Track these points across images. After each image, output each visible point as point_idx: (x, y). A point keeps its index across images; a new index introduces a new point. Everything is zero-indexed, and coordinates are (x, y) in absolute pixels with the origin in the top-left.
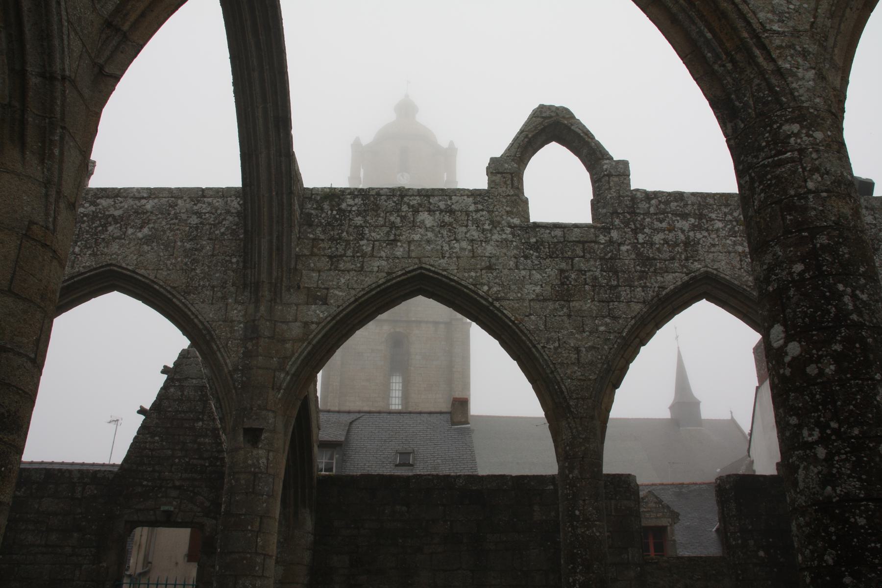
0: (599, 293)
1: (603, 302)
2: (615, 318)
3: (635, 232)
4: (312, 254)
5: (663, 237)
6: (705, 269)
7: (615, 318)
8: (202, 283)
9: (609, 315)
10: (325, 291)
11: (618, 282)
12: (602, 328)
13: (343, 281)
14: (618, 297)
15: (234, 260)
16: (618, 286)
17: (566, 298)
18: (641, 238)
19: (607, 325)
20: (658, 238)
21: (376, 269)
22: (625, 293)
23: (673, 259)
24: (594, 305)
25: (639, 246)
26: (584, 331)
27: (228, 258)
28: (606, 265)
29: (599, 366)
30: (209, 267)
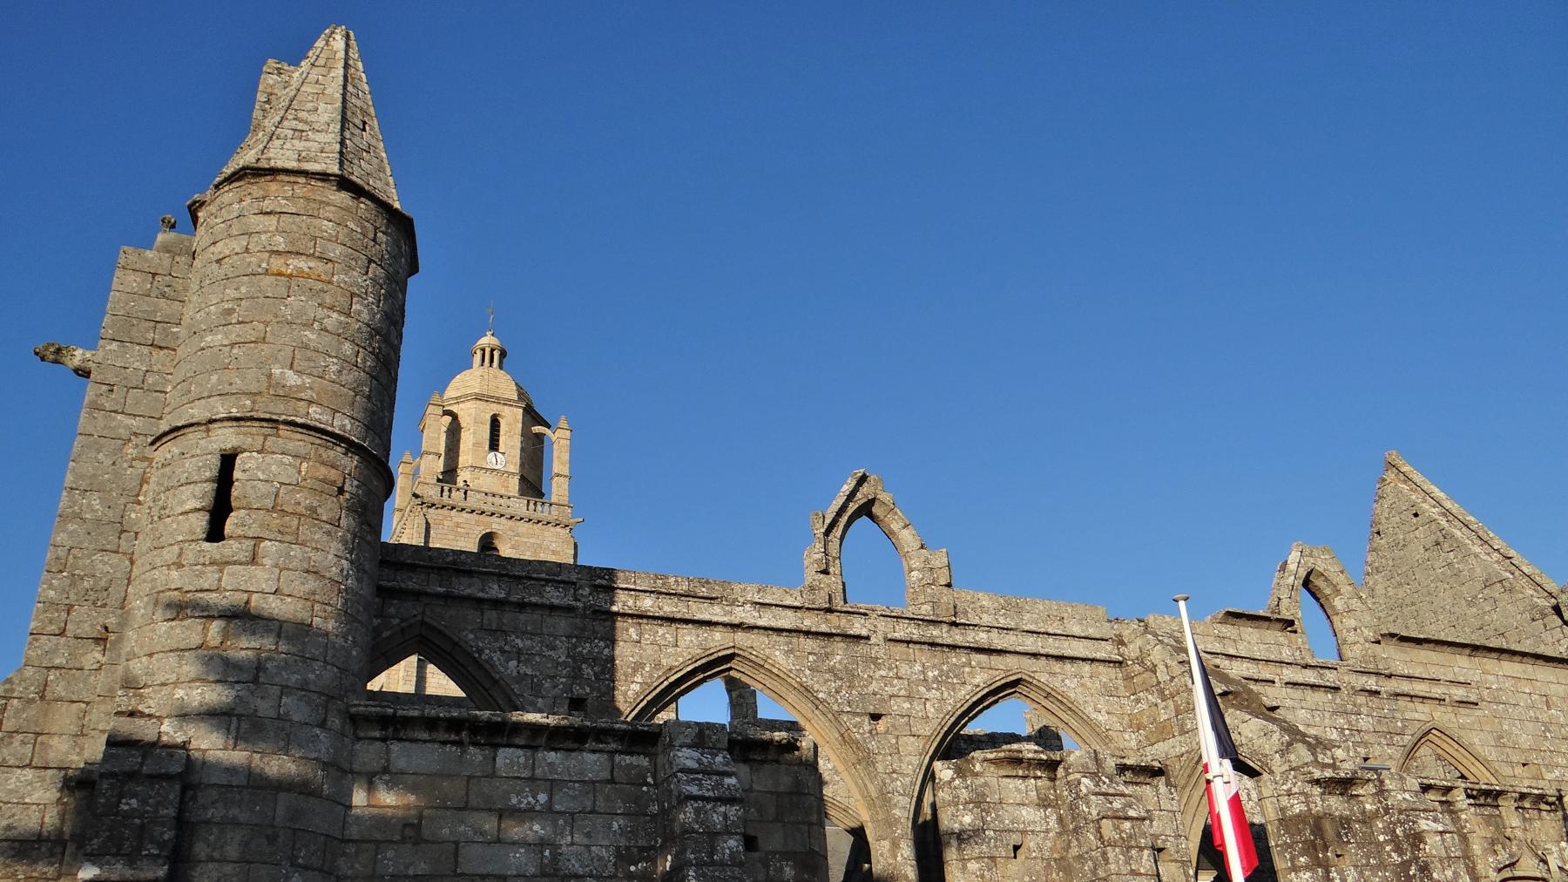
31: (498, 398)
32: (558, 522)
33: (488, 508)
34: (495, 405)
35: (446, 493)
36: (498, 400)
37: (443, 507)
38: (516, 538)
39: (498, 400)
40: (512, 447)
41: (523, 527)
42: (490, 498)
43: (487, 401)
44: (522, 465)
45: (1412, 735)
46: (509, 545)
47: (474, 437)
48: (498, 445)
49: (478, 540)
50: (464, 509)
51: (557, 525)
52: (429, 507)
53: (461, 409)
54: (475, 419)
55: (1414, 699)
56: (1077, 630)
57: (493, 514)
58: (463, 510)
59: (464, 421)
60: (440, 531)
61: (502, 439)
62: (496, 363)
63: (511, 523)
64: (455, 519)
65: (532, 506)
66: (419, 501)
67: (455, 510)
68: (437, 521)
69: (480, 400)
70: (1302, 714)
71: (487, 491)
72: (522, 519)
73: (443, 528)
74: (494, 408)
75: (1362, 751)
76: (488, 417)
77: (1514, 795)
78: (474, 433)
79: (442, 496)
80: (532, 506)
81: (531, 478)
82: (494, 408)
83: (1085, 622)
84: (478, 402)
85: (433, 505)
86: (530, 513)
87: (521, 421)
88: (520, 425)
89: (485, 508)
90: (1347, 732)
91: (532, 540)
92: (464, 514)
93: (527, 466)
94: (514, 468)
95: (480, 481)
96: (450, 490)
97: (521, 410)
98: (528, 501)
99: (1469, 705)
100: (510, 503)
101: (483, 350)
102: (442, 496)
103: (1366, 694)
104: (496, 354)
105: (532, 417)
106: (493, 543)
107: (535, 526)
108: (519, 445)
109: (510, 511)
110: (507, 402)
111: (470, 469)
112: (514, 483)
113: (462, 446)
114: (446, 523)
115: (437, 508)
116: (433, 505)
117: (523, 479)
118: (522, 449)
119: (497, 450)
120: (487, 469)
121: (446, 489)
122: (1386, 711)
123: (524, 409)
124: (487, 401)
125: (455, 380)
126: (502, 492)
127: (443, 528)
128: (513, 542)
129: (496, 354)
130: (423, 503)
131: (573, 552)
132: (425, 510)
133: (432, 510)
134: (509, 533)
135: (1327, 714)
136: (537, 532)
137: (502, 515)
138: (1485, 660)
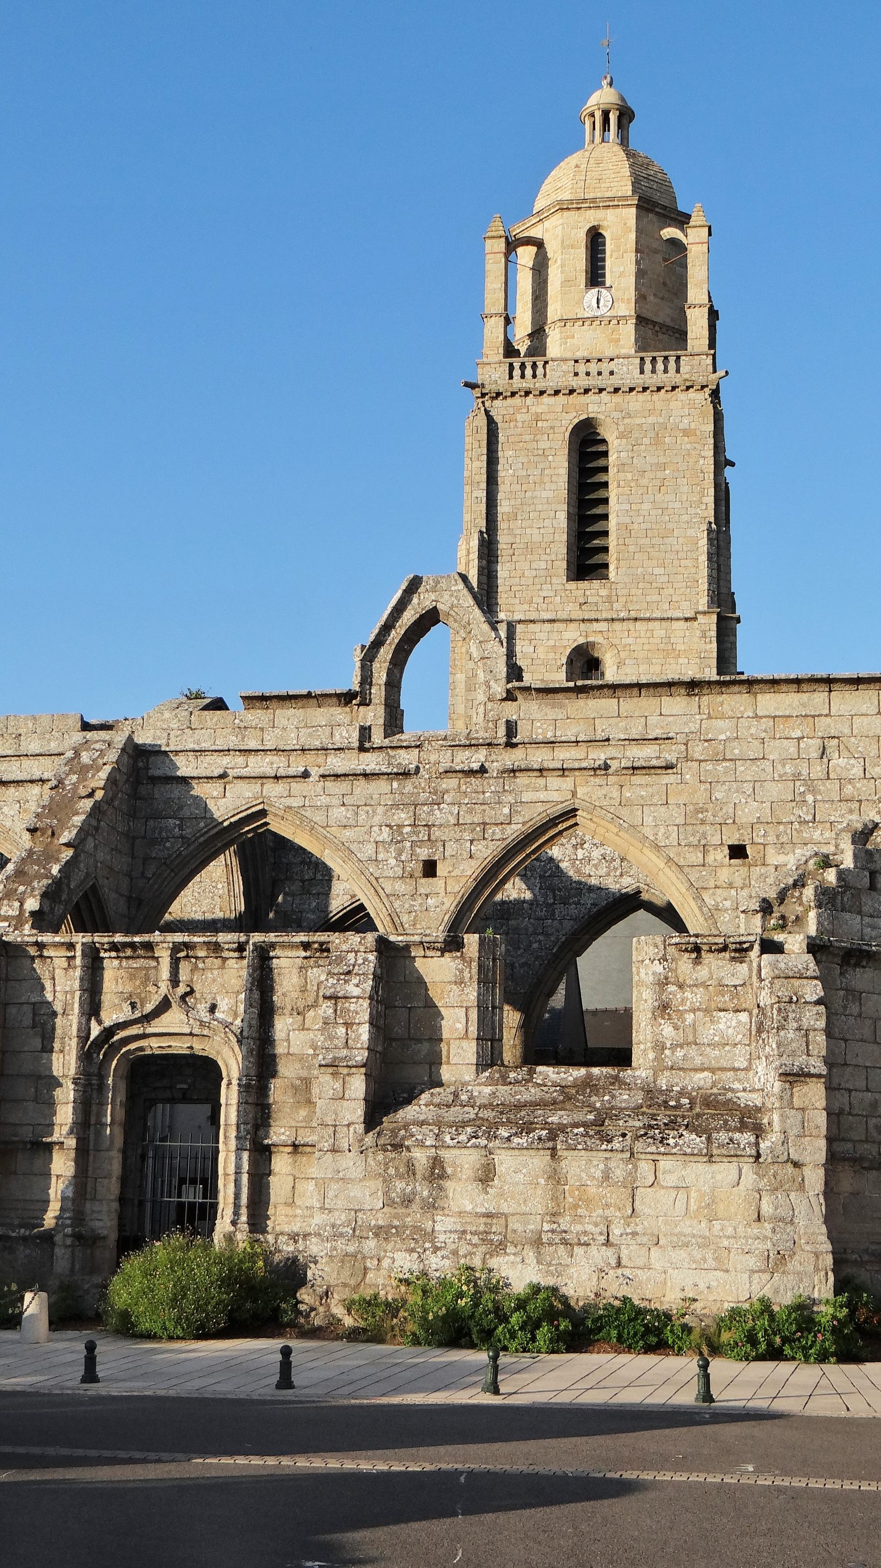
0: (535, 912)
1: (539, 919)
2: (547, 935)
3: (575, 847)
4: (286, 879)
5: (603, 851)
6: (638, 884)
7: (547, 935)
8: (194, 909)
9: (542, 933)
10: (300, 914)
11: (555, 900)
12: (535, 946)
13: (314, 904)
14: (553, 914)
15: (220, 886)
16: (554, 904)
17: (506, 917)
18: (580, 853)
19: (540, 942)
20: (596, 854)
21: (342, 892)
22: (559, 910)
23: (608, 875)
24: (531, 924)
25: (578, 862)
26: (519, 948)
27: (214, 884)
28: (545, 883)
29: (530, 980)
30: (199, 893)
31: (594, 200)
32: (688, 384)
33: (582, 382)
34: (592, 211)
35: (517, 372)
36: (594, 204)
37: (513, 394)
38: (626, 421)
39: (594, 204)
40: (622, 275)
41: (636, 401)
42: (582, 368)
43: (579, 208)
44: (641, 298)
45: (524, 824)
46: (616, 433)
47: (562, 273)
48: (604, 275)
49: (567, 435)
50: (544, 392)
51: (688, 388)
52: (493, 398)
53: (547, 230)
54: (563, 242)
55: (545, 773)
56: (34, 747)
57: (587, 391)
58: (542, 393)
59: (551, 248)
60: (511, 432)
61: (609, 264)
62: (598, 139)
63: (618, 398)
64: (533, 409)
65: (648, 366)
66: (477, 392)
67: (531, 396)
68: (507, 417)
69: (568, 209)
70: (339, 813)
71: (586, 354)
72: (632, 390)
73: (516, 426)
74: (590, 218)
75: (424, 853)
76: (581, 237)
77: (165, 945)
78: (562, 266)
79: (511, 377)
80: (648, 366)
81: (663, 316)
82: (590, 218)
83: (47, 736)
84: (566, 213)
85: (498, 394)
86: (649, 379)
87: (634, 228)
88: (633, 236)
89: (574, 383)
90: (407, 829)
91: (651, 420)
92: (545, 399)
93: (651, 298)
94: (627, 308)
95: (575, 341)
96: (534, 366)
97: (633, 210)
98: (642, 359)
99: (653, 771)
100: (612, 366)
101: (592, 115)
102: (511, 377)
103: (460, 775)
104: (613, 117)
105: (657, 214)
106: (599, 434)
107: (656, 396)
108: (632, 268)
109: (615, 381)
110: (611, 203)
111: (559, 324)
112: (629, 330)
113: (549, 288)
114: (519, 417)
115: (505, 398)
116: (498, 394)
117: (641, 320)
118: (640, 274)
119: (602, 284)
120: (584, 320)
121: (517, 365)
122: (487, 795)
123: (638, 207)
124: (579, 208)
125: (549, 179)
126: (609, 353)
127: (516, 426)
128: (621, 428)
129: (613, 117)
130: (483, 395)
131: (711, 427)
132: (487, 404)
133: (498, 403)
134: (616, 415)
135: (380, 810)
136: (659, 405)
137: (601, 390)
138: (720, 698)
